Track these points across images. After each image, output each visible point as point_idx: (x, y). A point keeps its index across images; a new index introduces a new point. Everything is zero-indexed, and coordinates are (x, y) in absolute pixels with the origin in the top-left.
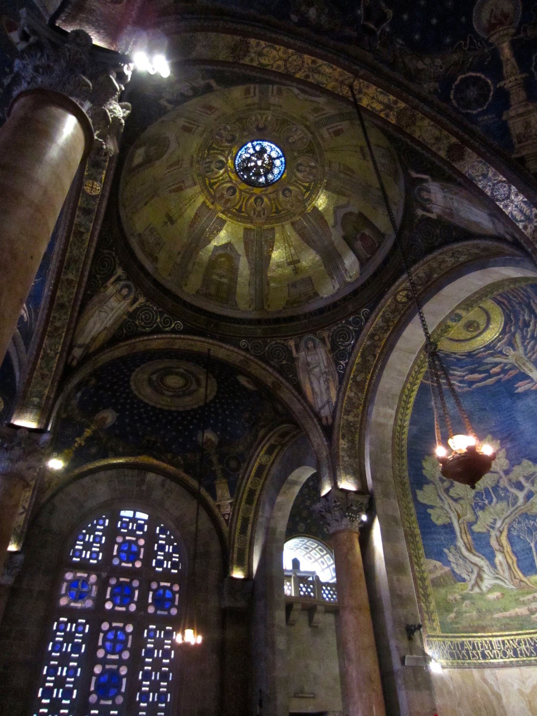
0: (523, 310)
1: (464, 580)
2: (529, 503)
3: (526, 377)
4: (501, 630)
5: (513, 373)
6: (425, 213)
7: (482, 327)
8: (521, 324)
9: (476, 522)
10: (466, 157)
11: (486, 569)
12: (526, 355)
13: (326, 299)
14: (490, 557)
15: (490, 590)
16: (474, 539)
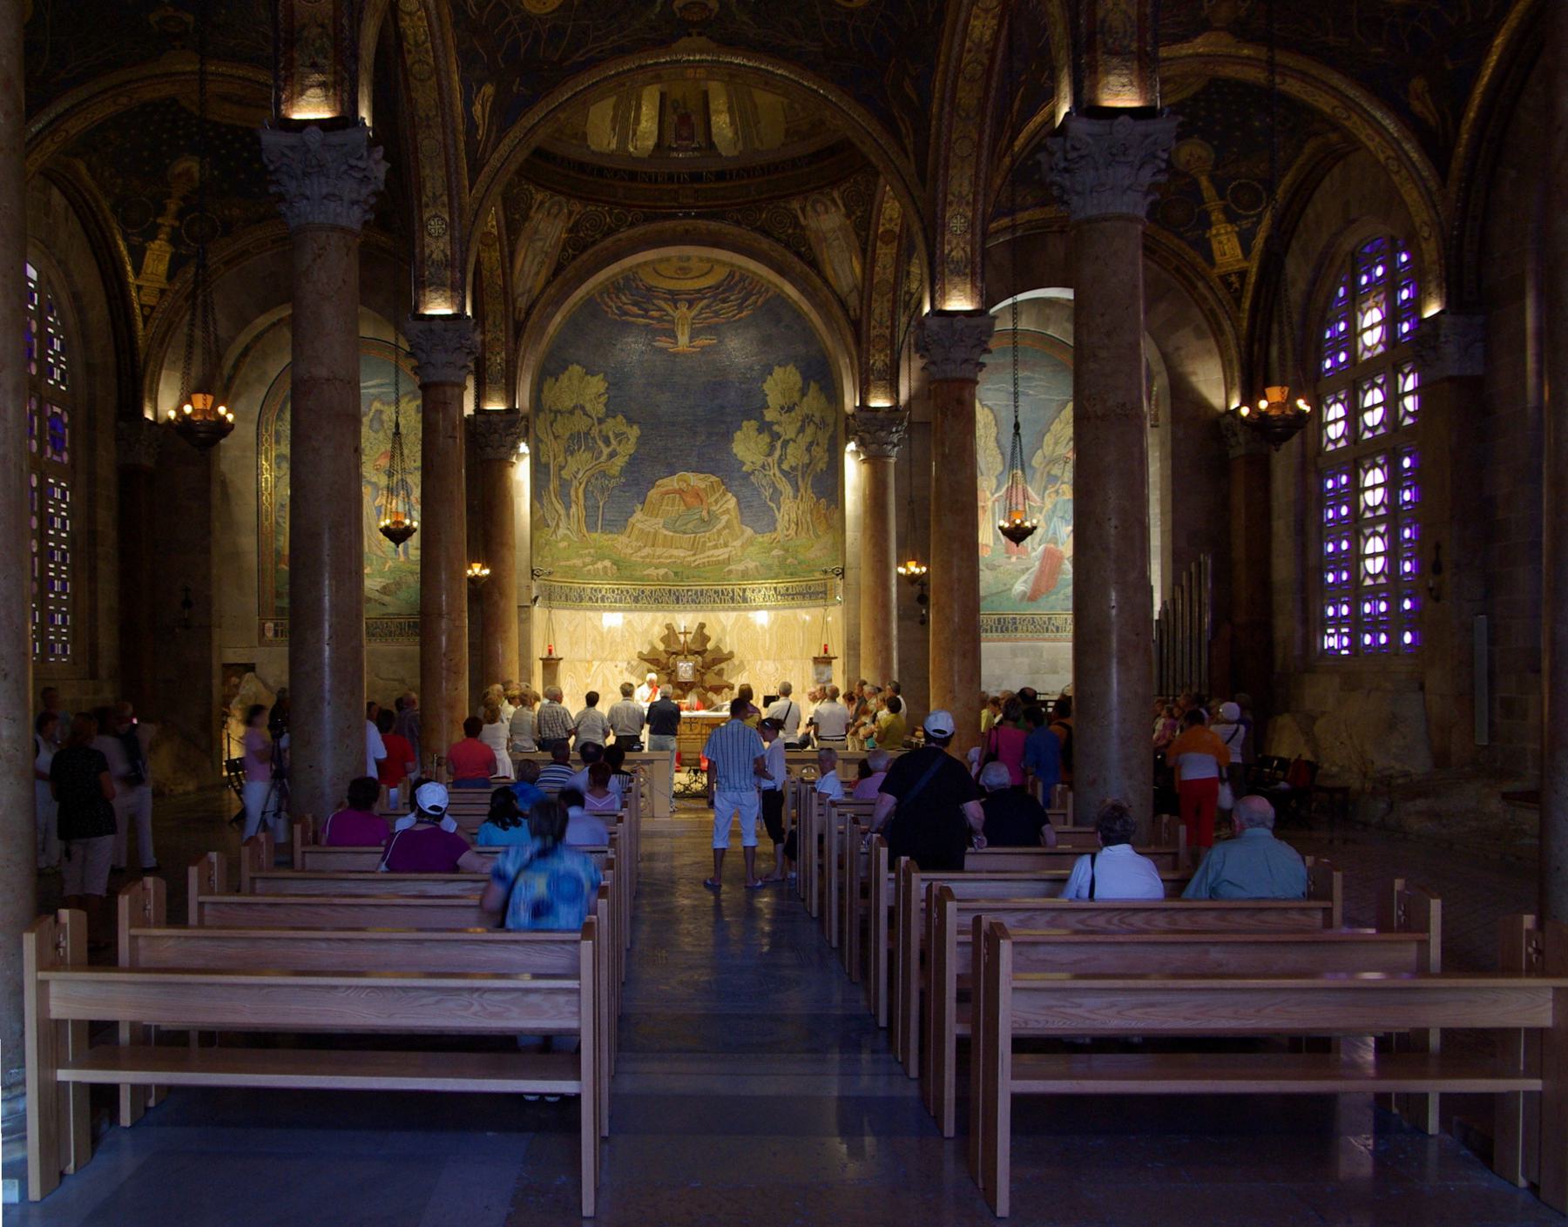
0: (739, 293)
1: (548, 526)
2: (610, 463)
3: (675, 337)
4: (563, 577)
5: (667, 326)
6: (799, 212)
7: (689, 276)
8: (720, 297)
9: (564, 467)
10: (890, 246)
11: (562, 518)
12: (693, 319)
13: (593, 152)
14: (568, 507)
15: (562, 540)
16: (561, 485)
